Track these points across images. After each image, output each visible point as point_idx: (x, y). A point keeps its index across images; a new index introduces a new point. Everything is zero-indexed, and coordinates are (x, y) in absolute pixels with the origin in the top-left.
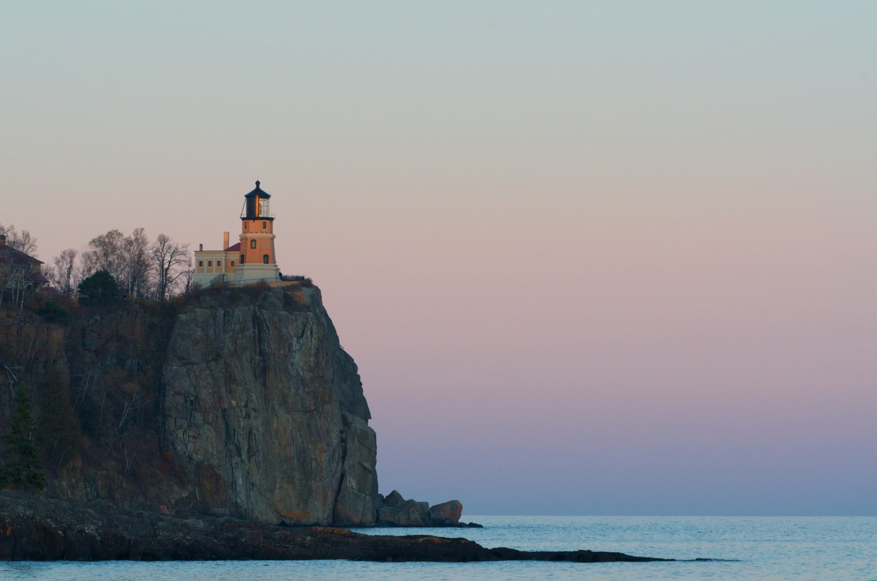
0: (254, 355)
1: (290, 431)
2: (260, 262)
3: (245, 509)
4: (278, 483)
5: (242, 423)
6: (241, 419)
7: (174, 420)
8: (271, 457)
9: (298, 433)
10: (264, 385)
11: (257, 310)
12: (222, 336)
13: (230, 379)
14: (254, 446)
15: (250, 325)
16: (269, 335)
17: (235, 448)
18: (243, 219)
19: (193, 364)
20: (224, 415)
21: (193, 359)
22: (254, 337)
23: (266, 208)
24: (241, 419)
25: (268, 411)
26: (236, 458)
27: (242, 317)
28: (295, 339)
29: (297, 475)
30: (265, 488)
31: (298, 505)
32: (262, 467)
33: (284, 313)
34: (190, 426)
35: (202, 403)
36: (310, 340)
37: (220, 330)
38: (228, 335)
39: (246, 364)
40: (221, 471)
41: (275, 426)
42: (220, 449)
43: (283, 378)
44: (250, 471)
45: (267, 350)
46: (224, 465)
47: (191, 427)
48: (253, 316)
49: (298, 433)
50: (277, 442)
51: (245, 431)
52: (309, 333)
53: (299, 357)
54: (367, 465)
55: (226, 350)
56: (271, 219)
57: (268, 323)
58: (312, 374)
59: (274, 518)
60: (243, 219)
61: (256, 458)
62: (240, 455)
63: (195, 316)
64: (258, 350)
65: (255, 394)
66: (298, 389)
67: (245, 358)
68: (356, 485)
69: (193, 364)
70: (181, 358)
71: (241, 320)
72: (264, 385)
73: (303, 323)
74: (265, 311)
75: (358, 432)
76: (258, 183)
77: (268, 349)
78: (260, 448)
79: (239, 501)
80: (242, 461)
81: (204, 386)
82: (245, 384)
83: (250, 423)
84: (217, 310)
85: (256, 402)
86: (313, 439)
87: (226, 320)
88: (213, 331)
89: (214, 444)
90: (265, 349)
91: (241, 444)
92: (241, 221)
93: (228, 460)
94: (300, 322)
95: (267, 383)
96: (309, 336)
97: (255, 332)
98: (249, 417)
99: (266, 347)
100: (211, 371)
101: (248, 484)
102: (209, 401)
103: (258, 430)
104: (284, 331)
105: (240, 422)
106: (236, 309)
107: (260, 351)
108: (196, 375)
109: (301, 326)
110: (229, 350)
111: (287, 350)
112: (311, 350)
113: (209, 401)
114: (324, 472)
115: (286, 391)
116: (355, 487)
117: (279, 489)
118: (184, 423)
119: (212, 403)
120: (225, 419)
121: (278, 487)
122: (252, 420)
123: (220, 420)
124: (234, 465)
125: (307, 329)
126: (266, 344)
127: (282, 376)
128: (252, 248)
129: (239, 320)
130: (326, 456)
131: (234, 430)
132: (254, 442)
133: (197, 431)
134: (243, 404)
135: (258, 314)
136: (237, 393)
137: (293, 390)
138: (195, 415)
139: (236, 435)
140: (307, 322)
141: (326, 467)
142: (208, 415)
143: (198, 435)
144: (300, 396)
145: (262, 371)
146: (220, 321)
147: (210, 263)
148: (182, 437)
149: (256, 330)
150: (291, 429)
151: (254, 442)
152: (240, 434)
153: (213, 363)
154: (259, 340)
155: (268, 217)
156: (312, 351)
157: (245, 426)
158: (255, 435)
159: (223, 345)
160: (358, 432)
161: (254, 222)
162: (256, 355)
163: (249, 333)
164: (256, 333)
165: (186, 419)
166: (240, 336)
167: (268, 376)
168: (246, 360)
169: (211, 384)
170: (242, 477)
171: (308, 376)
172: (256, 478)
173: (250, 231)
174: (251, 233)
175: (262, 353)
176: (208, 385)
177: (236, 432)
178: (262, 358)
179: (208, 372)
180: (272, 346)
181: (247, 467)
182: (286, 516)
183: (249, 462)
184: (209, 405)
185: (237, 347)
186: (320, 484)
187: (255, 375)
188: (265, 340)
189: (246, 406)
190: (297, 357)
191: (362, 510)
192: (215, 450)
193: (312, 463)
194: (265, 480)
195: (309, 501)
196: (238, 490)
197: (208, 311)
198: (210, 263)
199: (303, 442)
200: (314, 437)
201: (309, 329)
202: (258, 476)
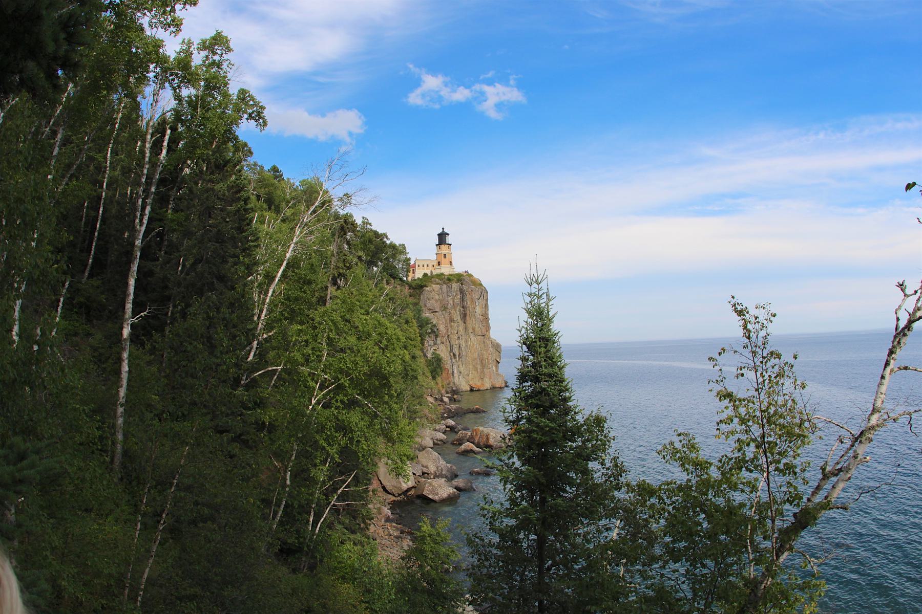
10: (465, 323)
13: (452, 320)
18: (437, 245)
21: (437, 310)
23: (449, 240)
29: (479, 367)
33: (473, 287)
34: (435, 344)
38: (450, 298)
39: (458, 313)
54: (498, 360)
55: (449, 305)
56: (450, 245)
70: (430, 309)
72: (465, 323)
76: (443, 229)
80: (456, 361)
145: (464, 316)
147: (423, 266)
153: (444, 312)
154: (463, 300)
163: (459, 297)
171: (482, 318)
172: (462, 369)
175: (463, 307)
189: (457, 333)
198: (423, 266)
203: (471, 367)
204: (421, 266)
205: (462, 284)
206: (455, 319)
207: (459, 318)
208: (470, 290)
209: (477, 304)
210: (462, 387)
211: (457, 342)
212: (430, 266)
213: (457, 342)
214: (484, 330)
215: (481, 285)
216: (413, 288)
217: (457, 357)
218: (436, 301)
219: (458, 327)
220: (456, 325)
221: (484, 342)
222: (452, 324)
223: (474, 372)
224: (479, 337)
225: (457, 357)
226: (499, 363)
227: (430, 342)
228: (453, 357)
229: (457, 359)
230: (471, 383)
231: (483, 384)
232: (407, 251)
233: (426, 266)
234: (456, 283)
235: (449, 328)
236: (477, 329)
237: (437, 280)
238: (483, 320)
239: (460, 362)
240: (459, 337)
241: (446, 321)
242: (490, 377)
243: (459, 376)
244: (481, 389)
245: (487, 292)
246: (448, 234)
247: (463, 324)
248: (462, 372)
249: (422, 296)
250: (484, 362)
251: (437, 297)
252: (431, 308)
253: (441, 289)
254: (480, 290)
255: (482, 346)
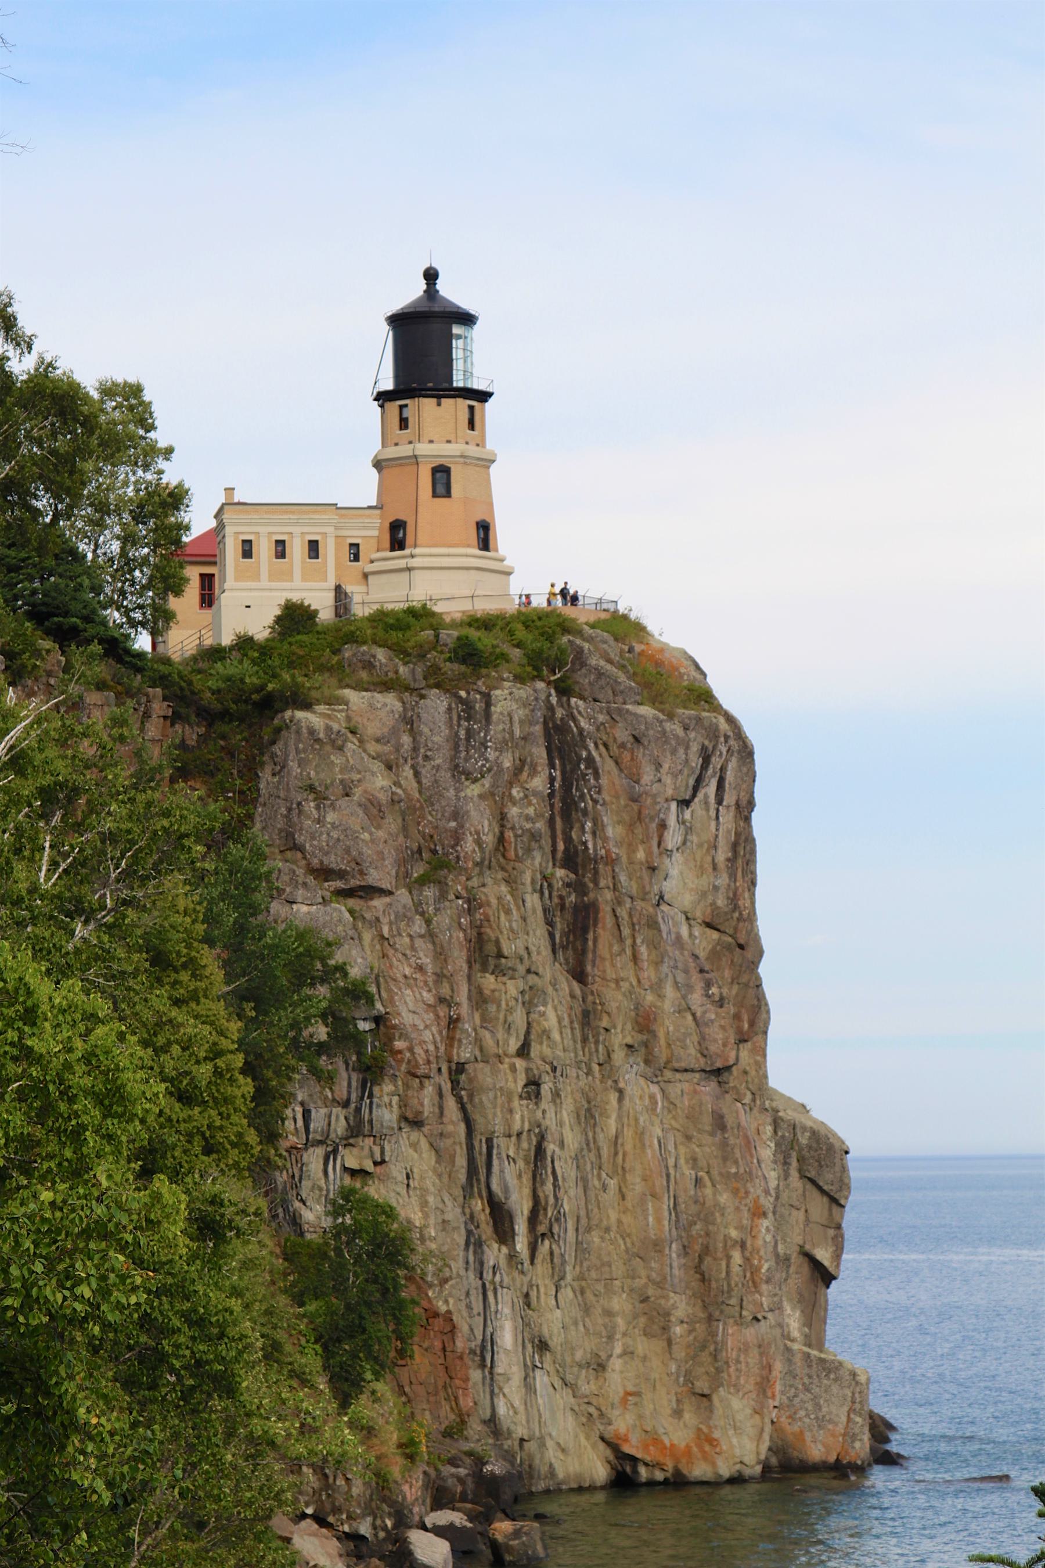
0: (551, 864)
1: (656, 1142)
2: (469, 546)
3: (522, 1440)
4: (618, 1336)
5: (518, 1117)
6: (516, 1103)
7: (299, 1109)
8: (596, 1240)
9: (682, 1150)
10: (579, 975)
11: (554, 700)
12: (452, 792)
14: (551, 1200)
15: (539, 753)
16: (599, 792)
17: (488, 1211)
18: (382, 398)
19: (371, 891)
20: (455, 1084)
21: (375, 877)
22: (551, 796)
24: (516, 1103)
25: (589, 1072)
26: (496, 1246)
27: (521, 722)
28: (674, 806)
29: (681, 1306)
30: (579, 1355)
31: (678, 1413)
32: (569, 1277)
33: (646, 711)
34: (356, 1130)
35: (399, 1044)
36: (713, 813)
37: (438, 768)
38: (473, 790)
39: (533, 900)
40: (451, 1301)
41: (612, 1124)
42: (449, 1216)
43: (643, 950)
44: (533, 1294)
45: (590, 845)
46: (458, 1275)
47: (357, 1136)
48: (545, 723)
49: (682, 1150)
50: (612, 1183)
51: (525, 1145)
52: (711, 789)
53: (681, 873)
54: (823, 1255)
55: (469, 845)
56: (483, 396)
57: (592, 746)
58: (715, 935)
59: (599, 1464)
60: (382, 398)
61: (554, 1247)
62: (504, 1233)
63: (349, 719)
64: (561, 846)
65: (555, 1009)
66: (690, 988)
67: (527, 878)
68: (800, 1330)
69: (371, 891)
70: (324, 873)
71: (517, 733)
73: (704, 748)
74: (581, 703)
75: (804, 1140)
76: (431, 276)
77: (595, 845)
78: (566, 1207)
79: (502, 1410)
80: (512, 1256)
81: (405, 977)
82: (529, 971)
83: (539, 1114)
84: (423, 697)
85: (556, 1036)
86: (733, 1170)
87: (462, 734)
88: (412, 772)
89: (431, 1199)
90: (585, 843)
91: (514, 1197)
92: (375, 408)
93: (471, 1258)
94: (695, 748)
95: (589, 968)
96: (712, 799)
97: (552, 780)
98: (538, 1095)
99: (588, 837)
100: (428, 922)
101: (529, 1346)
102: (427, 1036)
103: (562, 1144)
104: (647, 778)
105: (511, 1111)
106: (498, 692)
107: (566, 850)
108: (382, 937)
109: (696, 762)
110: (478, 842)
111: (655, 849)
112: (715, 847)
113: (427, 1036)
114: (764, 1287)
115: (650, 998)
116: (796, 1334)
117: (620, 1356)
118: (337, 1117)
119: (435, 1043)
120: (460, 1100)
121: (618, 1350)
122: (544, 1105)
123: (451, 1103)
124: (488, 1276)
125: (710, 771)
126: (589, 825)
127: (639, 941)
128: (435, 495)
129: (511, 733)
130: (768, 1230)
131: (489, 1141)
132: (549, 1186)
133: (377, 1150)
134: (514, 1045)
135: (560, 713)
136: (499, 1006)
137: (669, 991)
138: (376, 1090)
139: (495, 1162)
140: (714, 747)
141: (768, 1270)
142: (422, 1086)
143: (376, 1164)
144: (694, 1015)
146: (436, 739)
147: (281, 549)
148: (321, 1174)
149: (557, 774)
150: (660, 1134)
151: (549, 1186)
152: (508, 1156)
153: (430, 893)
155: (469, 386)
156: (720, 851)
157: (526, 1127)
158: (553, 1162)
159: (453, 824)
160: (804, 1140)
161: (439, 404)
162: (554, 865)
163: (539, 783)
164: (557, 785)
165: (346, 1104)
166: (514, 792)
167: (590, 943)
168: (533, 882)
169: (430, 969)
170: (514, 1320)
171: (704, 941)
173: (425, 438)
174: (431, 442)
175: (573, 859)
176: (418, 976)
177: (495, 1152)
178: (573, 876)
179: (418, 926)
180: (610, 832)
181: (526, 1279)
182: (639, 1456)
183: (532, 1263)
184: (427, 1051)
185: (509, 835)
186: (750, 1333)
187: (551, 935)
188: (585, 812)
189: (523, 1051)
190: (674, 872)
191: (844, 1419)
192: (432, 1221)
193: (729, 1258)
194: (581, 1328)
195: (715, 1399)
196: (499, 1369)
197: (390, 701)
198: (281, 549)
199: (698, 1182)
200: (736, 1162)
201: (715, 773)
202: (558, 1313)
203: (620, 1303)
204: (264, 550)
205: (564, 690)
206: (507, 948)
207: (538, 938)
208: (622, 734)
209: (673, 838)
210: (552, 1453)
211: (521, 1116)
212: (329, 550)
213: (521, 1116)
214: (719, 1035)
215: (704, 697)
216: (209, 717)
217: (521, 1227)
218: (374, 810)
219: (529, 1007)
220: (514, 987)
221: (720, 1123)
222: (489, 981)
223: (642, 1346)
224: (681, 1087)
225: (521, 1227)
226: (825, 1276)
227: (318, 1116)
228: (486, 1230)
229: (521, 1245)
230: (622, 1423)
231: (706, 1440)
232: (161, 437)
233: (297, 550)
234: (519, 679)
235: (465, 1010)
236: (668, 1026)
237: (381, 655)
238: (714, 955)
239: (541, 1273)
240: (533, 1085)
241: (441, 955)
242: (764, 1386)
243: (530, 1369)
244: (699, 1471)
245: (746, 753)
246: (467, 319)
247: (566, 985)
248: (555, 1342)
249: (266, 778)
250: (716, 1269)
251: (380, 782)
252: (333, 861)
253: (410, 722)
254: (696, 740)
255: (707, 1147)
